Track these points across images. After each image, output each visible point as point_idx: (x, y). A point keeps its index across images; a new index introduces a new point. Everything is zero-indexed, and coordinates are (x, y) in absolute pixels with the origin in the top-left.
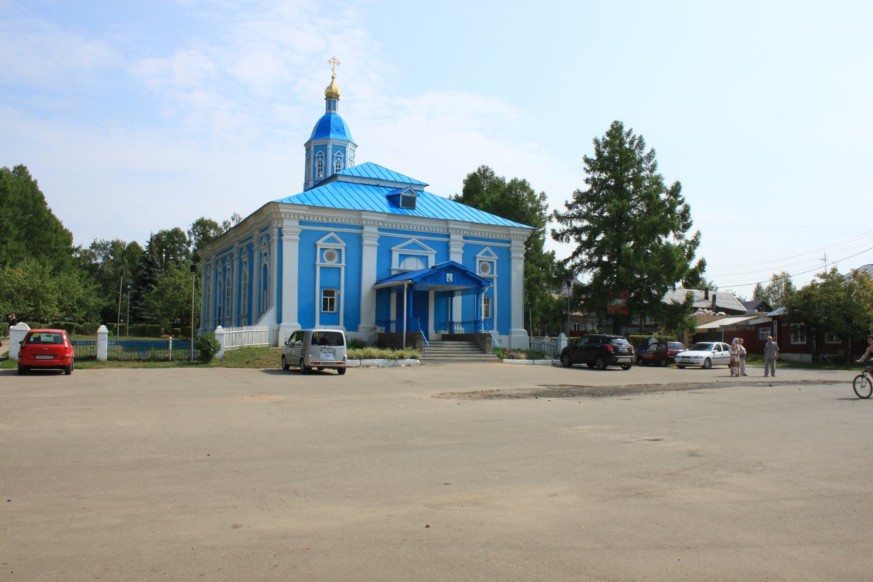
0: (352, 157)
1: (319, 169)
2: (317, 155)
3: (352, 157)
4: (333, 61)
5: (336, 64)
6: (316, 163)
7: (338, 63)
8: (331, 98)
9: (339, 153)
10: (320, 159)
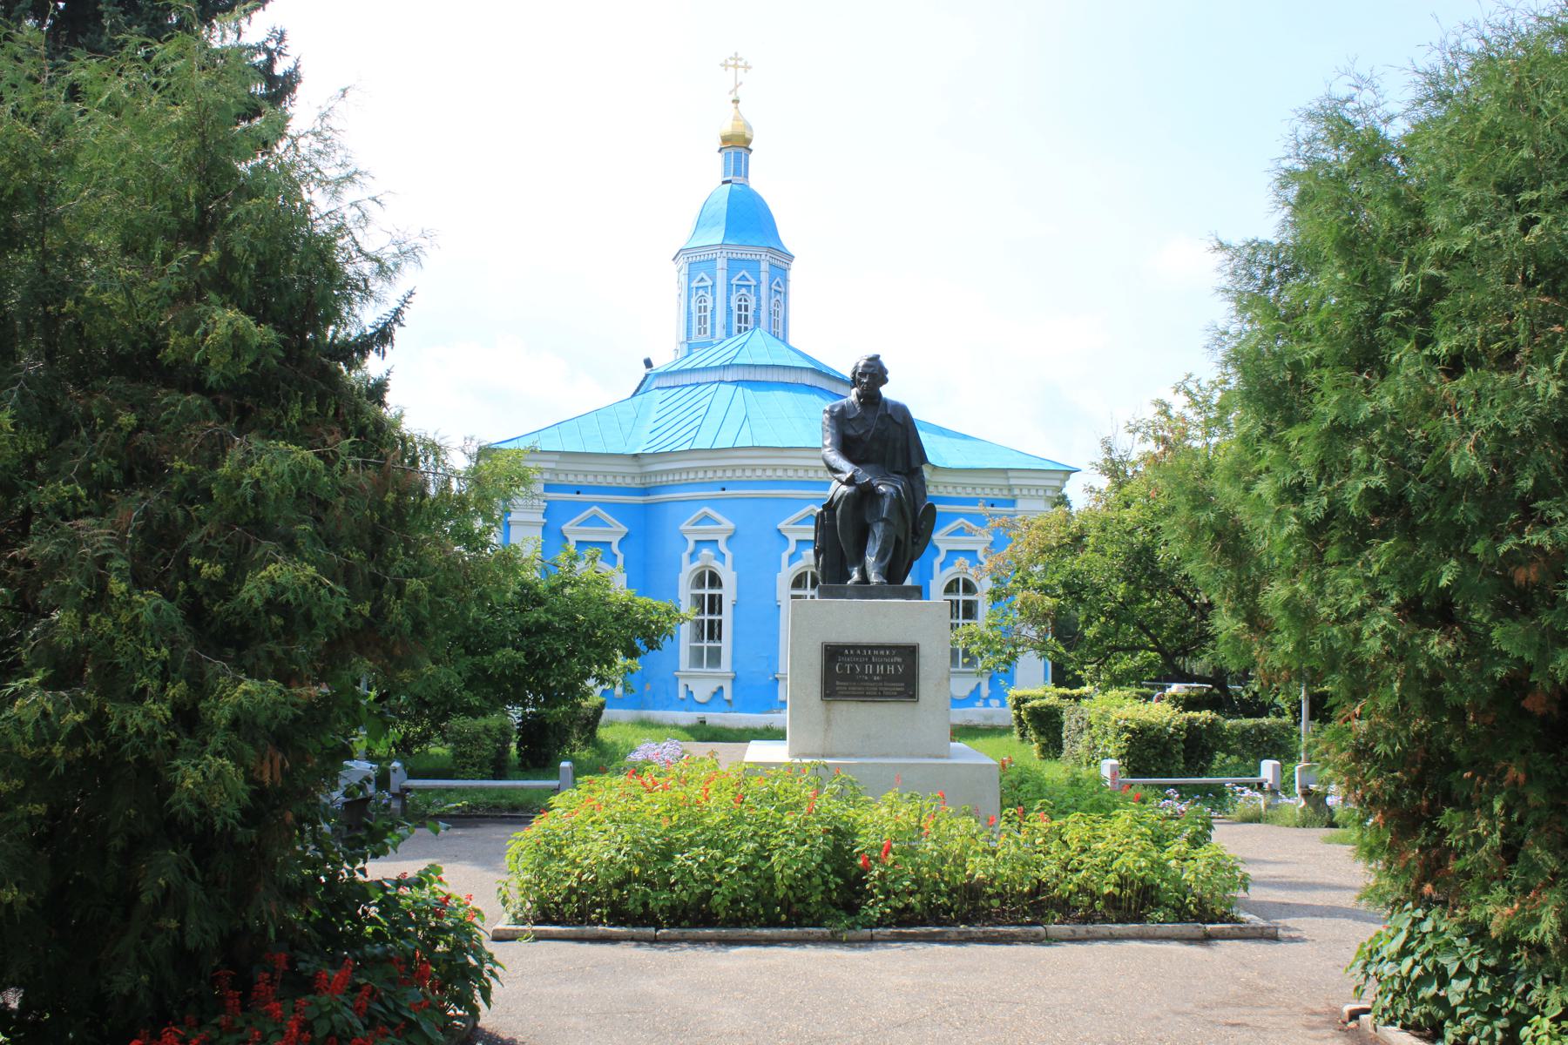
0: (778, 283)
2: (694, 284)
4: (733, 62)
5: (740, 70)
6: (693, 300)
7: (747, 67)
8: (737, 146)
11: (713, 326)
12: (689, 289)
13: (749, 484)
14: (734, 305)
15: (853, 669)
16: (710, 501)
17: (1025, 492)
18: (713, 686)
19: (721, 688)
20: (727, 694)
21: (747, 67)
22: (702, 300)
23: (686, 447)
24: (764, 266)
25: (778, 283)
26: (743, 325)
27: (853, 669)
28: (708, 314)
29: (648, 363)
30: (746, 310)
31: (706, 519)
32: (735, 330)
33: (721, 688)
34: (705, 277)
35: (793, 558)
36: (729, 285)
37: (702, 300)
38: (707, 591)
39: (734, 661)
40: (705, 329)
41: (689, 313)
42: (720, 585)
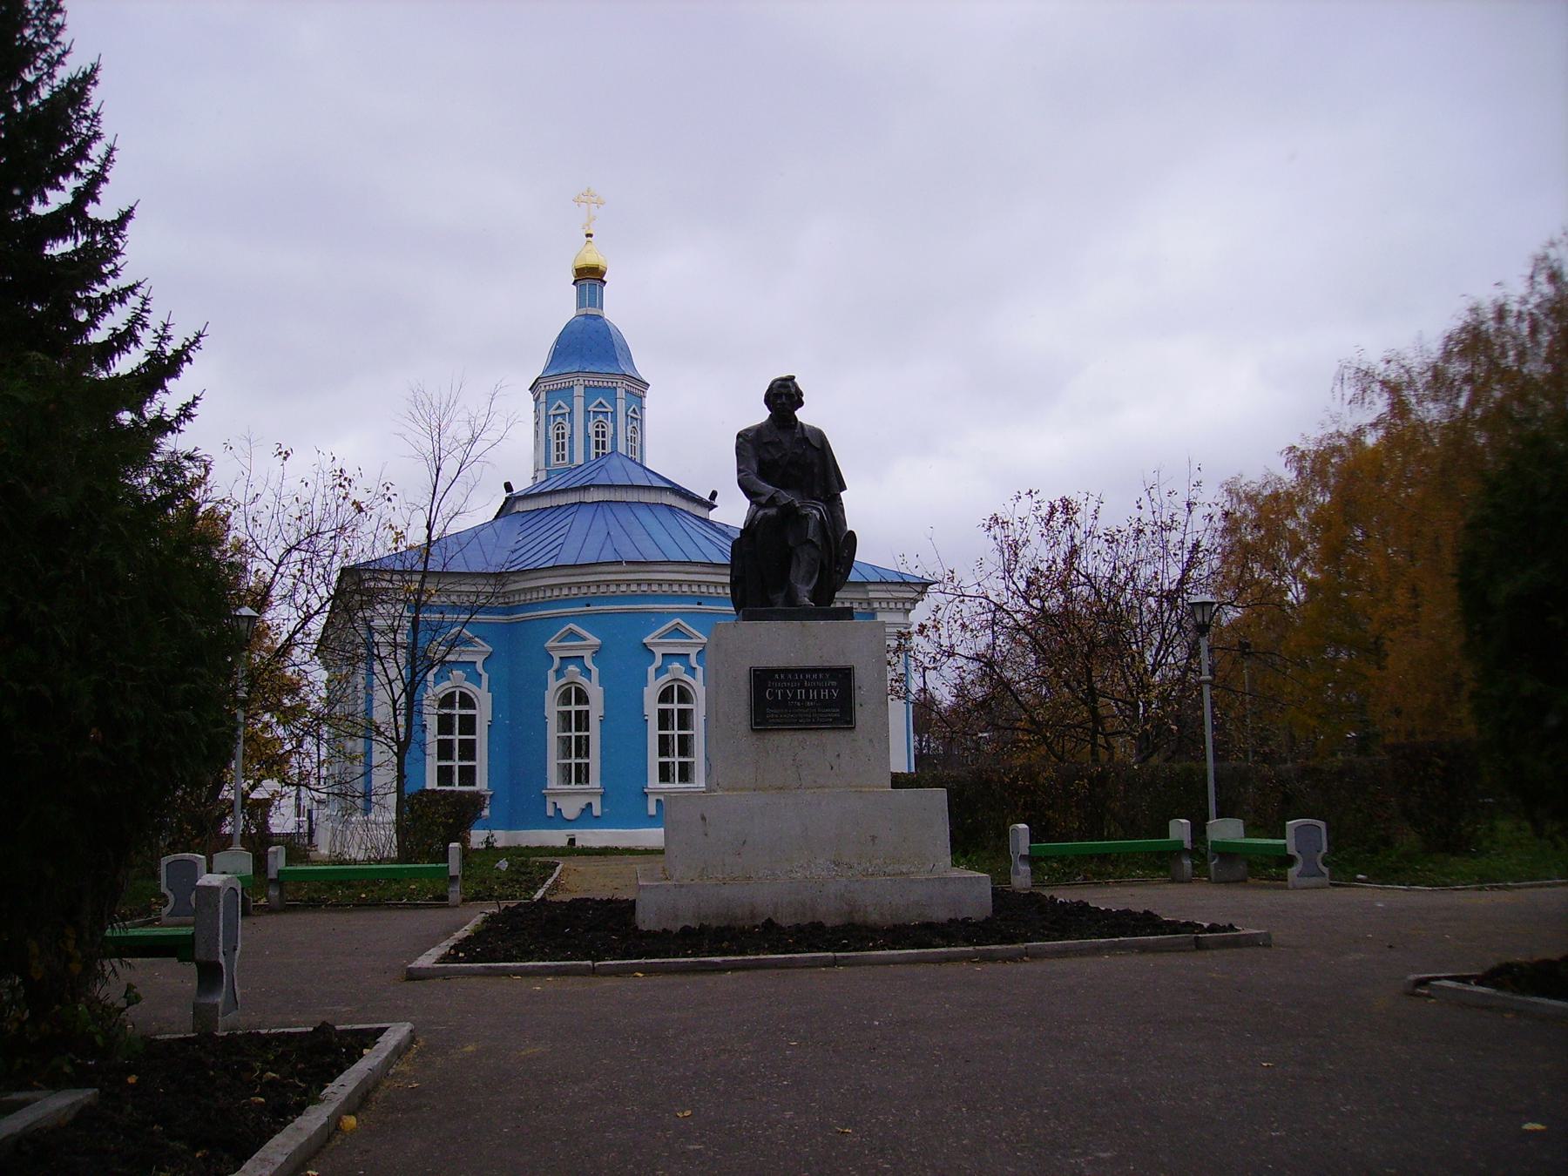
2: (551, 412)
3: (634, 411)
6: (551, 428)
7: (599, 203)
8: (590, 277)
9: (601, 403)
12: (547, 416)
13: (613, 599)
14: (592, 431)
15: (784, 695)
16: (575, 618)
17: (884, 605)
18: (581, 802)
19: (590, 805)
20: (597, 810)
21: (599, 203)
22: (560, 426)
23: (550, 564)
24: (621, 393)
25: (634, 411)
26: (601, 451)
27: (784, 695)
28: (566, 440)
29: (508, 487)
30: (604, 436)
31: (572, 635)
32: (593, 457)
33: (590, 805)
34: (563, 404)
35: (659, 672)
36: (587, 412)
37: (560, 426)
38: (573, 708)
39: (602, 778)
40: (563, 455)
42: (587, 702)
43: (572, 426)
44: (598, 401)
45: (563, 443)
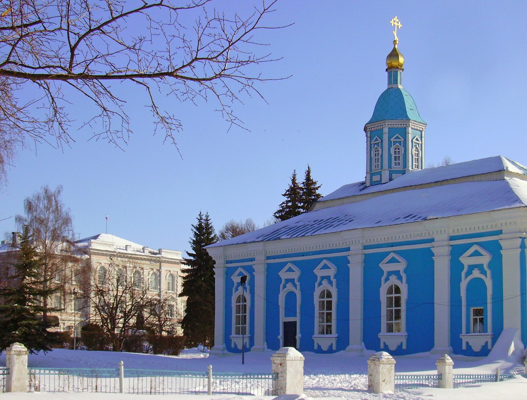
1: (376, 159)
3: (417, 140)
10: (397, 144)
11: (382, 163)
12: (371, 145)
14: (392, 151)
28: (380, 157)
30: (399, 154)
34: (378, 138)
41: (371, 158)
43: (382, 151)
44: (396, 136)
45: (378, 158)
